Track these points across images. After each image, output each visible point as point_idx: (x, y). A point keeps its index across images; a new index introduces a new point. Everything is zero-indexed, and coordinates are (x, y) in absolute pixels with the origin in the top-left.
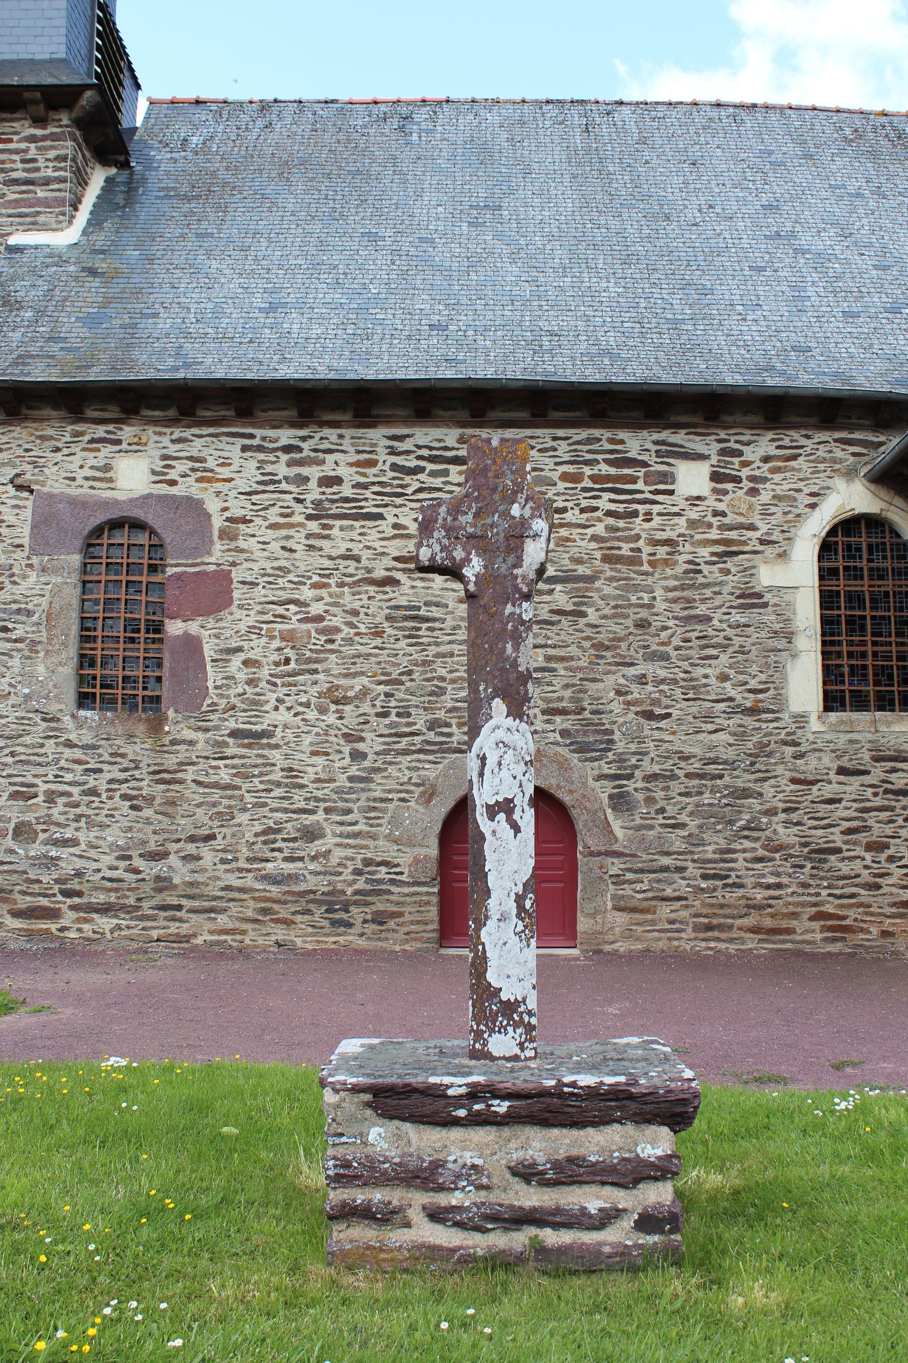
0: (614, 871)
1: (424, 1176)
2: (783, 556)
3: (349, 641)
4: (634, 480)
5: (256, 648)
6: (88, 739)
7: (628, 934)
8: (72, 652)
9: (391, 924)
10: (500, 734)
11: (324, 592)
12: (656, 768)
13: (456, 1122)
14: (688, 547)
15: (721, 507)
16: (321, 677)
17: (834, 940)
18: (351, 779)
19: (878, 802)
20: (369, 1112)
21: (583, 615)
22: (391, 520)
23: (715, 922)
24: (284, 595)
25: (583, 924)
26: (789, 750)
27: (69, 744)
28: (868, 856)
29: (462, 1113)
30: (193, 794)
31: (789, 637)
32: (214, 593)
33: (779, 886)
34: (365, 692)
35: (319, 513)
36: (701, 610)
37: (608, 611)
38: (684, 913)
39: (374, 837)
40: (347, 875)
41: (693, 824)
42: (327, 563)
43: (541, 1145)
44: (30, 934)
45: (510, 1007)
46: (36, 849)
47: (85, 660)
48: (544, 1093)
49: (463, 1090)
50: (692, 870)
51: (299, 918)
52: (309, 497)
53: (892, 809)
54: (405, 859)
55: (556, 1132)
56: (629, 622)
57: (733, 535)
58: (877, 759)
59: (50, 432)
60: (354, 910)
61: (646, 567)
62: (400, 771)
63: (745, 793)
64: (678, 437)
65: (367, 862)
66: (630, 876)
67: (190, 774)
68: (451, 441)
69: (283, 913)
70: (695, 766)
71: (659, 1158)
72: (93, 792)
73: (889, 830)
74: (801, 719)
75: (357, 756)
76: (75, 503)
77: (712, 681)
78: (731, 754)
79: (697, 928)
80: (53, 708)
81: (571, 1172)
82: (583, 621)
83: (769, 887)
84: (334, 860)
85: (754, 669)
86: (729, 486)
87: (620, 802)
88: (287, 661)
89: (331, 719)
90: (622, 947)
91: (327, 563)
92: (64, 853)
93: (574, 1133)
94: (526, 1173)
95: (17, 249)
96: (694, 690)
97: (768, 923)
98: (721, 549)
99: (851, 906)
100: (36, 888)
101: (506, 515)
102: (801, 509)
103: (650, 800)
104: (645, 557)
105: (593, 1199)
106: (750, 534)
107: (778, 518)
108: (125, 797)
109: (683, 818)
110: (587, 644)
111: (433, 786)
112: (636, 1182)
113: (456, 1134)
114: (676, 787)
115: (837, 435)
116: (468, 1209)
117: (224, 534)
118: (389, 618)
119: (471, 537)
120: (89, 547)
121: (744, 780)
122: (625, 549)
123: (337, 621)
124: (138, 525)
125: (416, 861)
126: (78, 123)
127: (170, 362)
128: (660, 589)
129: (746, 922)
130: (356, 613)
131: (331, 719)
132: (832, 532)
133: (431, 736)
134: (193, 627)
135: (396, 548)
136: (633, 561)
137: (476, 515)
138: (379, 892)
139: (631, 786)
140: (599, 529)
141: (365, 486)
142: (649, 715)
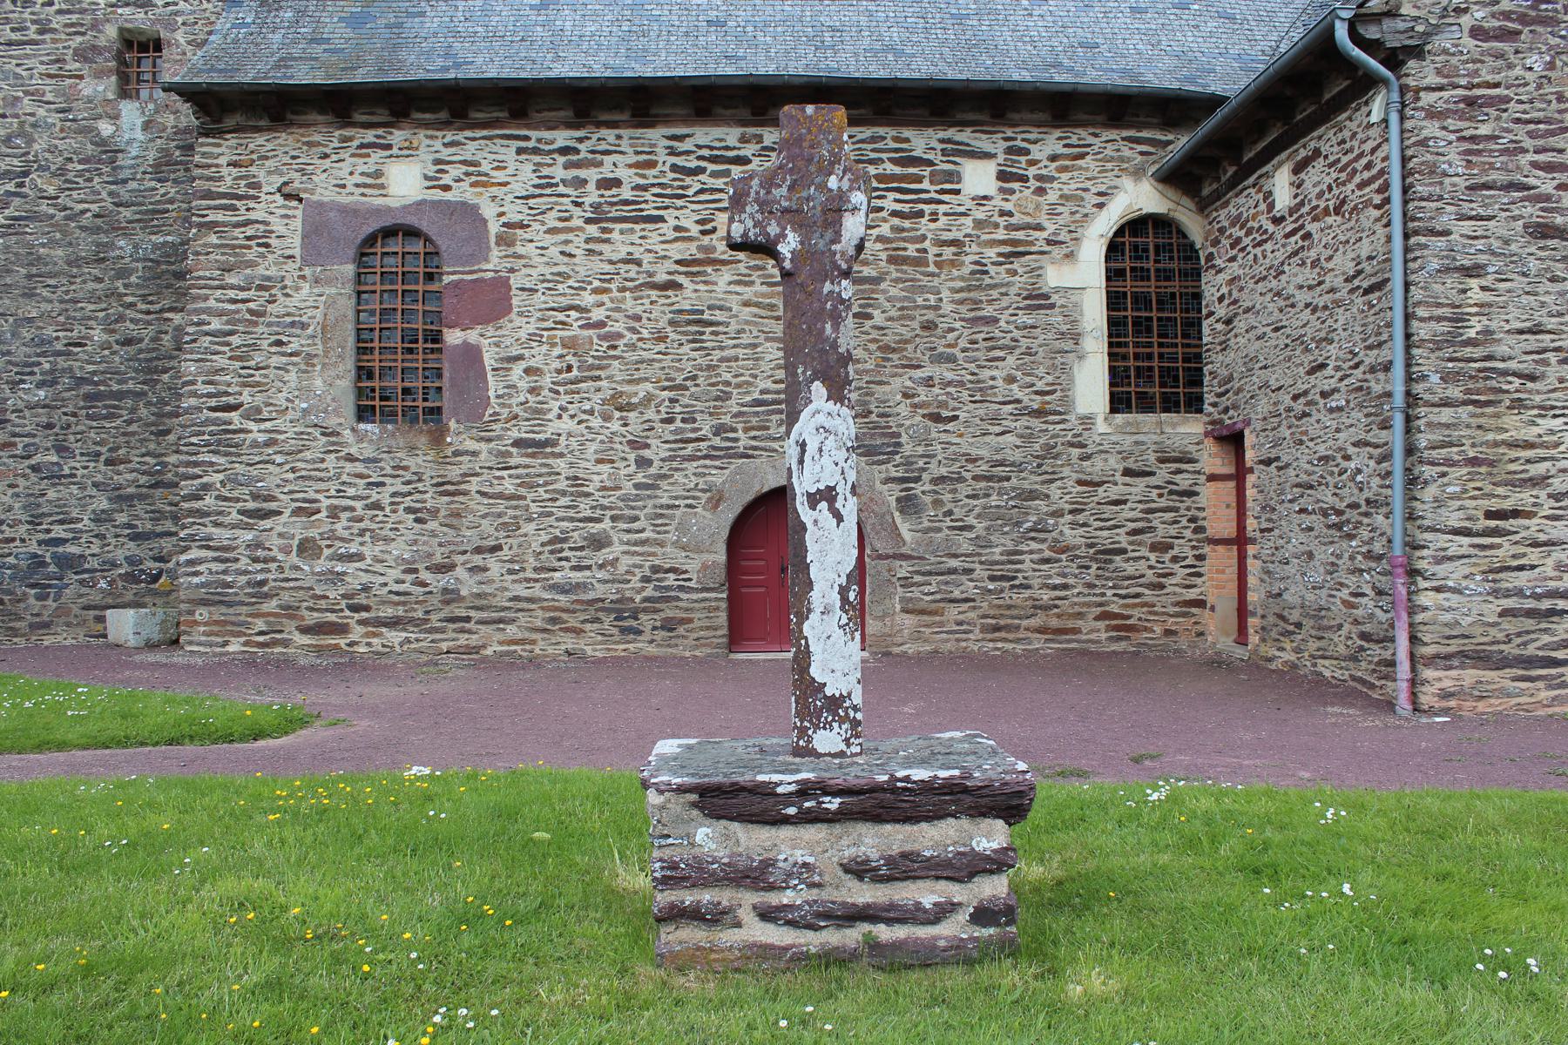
0: (902, 573)
1: (755, 876)
2: (1070, 256)
3: (632, 347)
4: (919, 179)
5: (538, 356)
6: (369, 452)
7: (917, 636)
8: (349, 364)
9: (681, 630)
10: (821, 419)
11: (605, 298)
12: (944, 471)
13: (786, 820)
14: (975, 248)
15: (1008, 206)
16: (604, 383)
17: (1119, 639)
18: (637, 486)
19: (1163, 503)
20: (695, 812)
21: (869, 317)
22: (672, 222)
23: (1002, 622)
24: (565, 301)
26: (1076, 452)
27: (350, 458)
28: (1153, 557)
29: (792, 811)
30: (478, 505)
31: (1076, 338)
32: (492, 301)
33: (1065, 587)
34: (649, 398)
35: (598, 216)
36: (988, 311)
37: (894, 313)
38: (972, 615)
39: (661, 544)
40: (635, 582)
41: (980, 527)
42: (608, 268)
43: (873, 841)
44: (319, 650)
45: (835, 703)
46: (321, 565)
47: (363, 373)
48: (876, 789)
49: (792, 788)
50: (980, 572)
51: (588, 626)
52: (588, 200)
53: (1176, 510)
55: (888, 827)
56: (915, 324)
57: (1020, 235)
58: (1162, 461)
59: (317, 138)
60: (643, 617)
61: (932, 268)
62: (687, 477)
63: (1032, 495)
64: (964, 135)
65: (656, 569)
66: (918, 578)
67: (474, 485)
68: (732, 141)
69: (573, 622)
71: (995, 851)
72: (377, 506)
73: (1173, 531)
74: (1087, 421)
75: (643, 463)
76: (344, 210)
77: (999, 383)
78: (1017, 456)
79: (984, 629)
80: (332, 422)
81: (905, 867)
82: (869, 323)
83: (1055, 587)
84: (622, 568)
85: (1041, 371)
86: (1016, 185)
87: (908, 505)
88: (569, 368)
89: (615, 426)
90: (910, 648)
91: (608, 268)
92: (350, 567)
93: (908, 828)
94: (858, 870)
96: (981, 393)
97: (1054, 623)
98: (1008, 249)
99: (1135, 606)
100: (323, 604)
101: (823, 187)
102: (1089, 209)
103: (937, 503)
104: (931, 258)
105: (927, 894)
106: (1037, 234)
107: (1065, 218)
108: (409, 510)
109: (971, 520)
110: (873, 347)
111: (720, 492)
112: (972, 875)
113: (786, 832)
114: (964, 489)
115: (1125, 133)
116: (799, 907)
117: (502, 240)
118: (672, 323)
119: (786, 211)
120: (363, 254)
121: (1031, 482)
123: (618, 327)
124: (412, 233)
125: (705, 567)
127: (440, 62)
128: (946, 290)
129: (1033, 622)
130: (638, 318)
131: (615, 426)
132: (1120, 232)
133: (717, 441)
134: (472, 336)
135: (677, 251)
136: (919, 262)
137: (791, 188)
138: (668, 599)
139: (918, 488)
141: (644, 188)
142: (936, 418)
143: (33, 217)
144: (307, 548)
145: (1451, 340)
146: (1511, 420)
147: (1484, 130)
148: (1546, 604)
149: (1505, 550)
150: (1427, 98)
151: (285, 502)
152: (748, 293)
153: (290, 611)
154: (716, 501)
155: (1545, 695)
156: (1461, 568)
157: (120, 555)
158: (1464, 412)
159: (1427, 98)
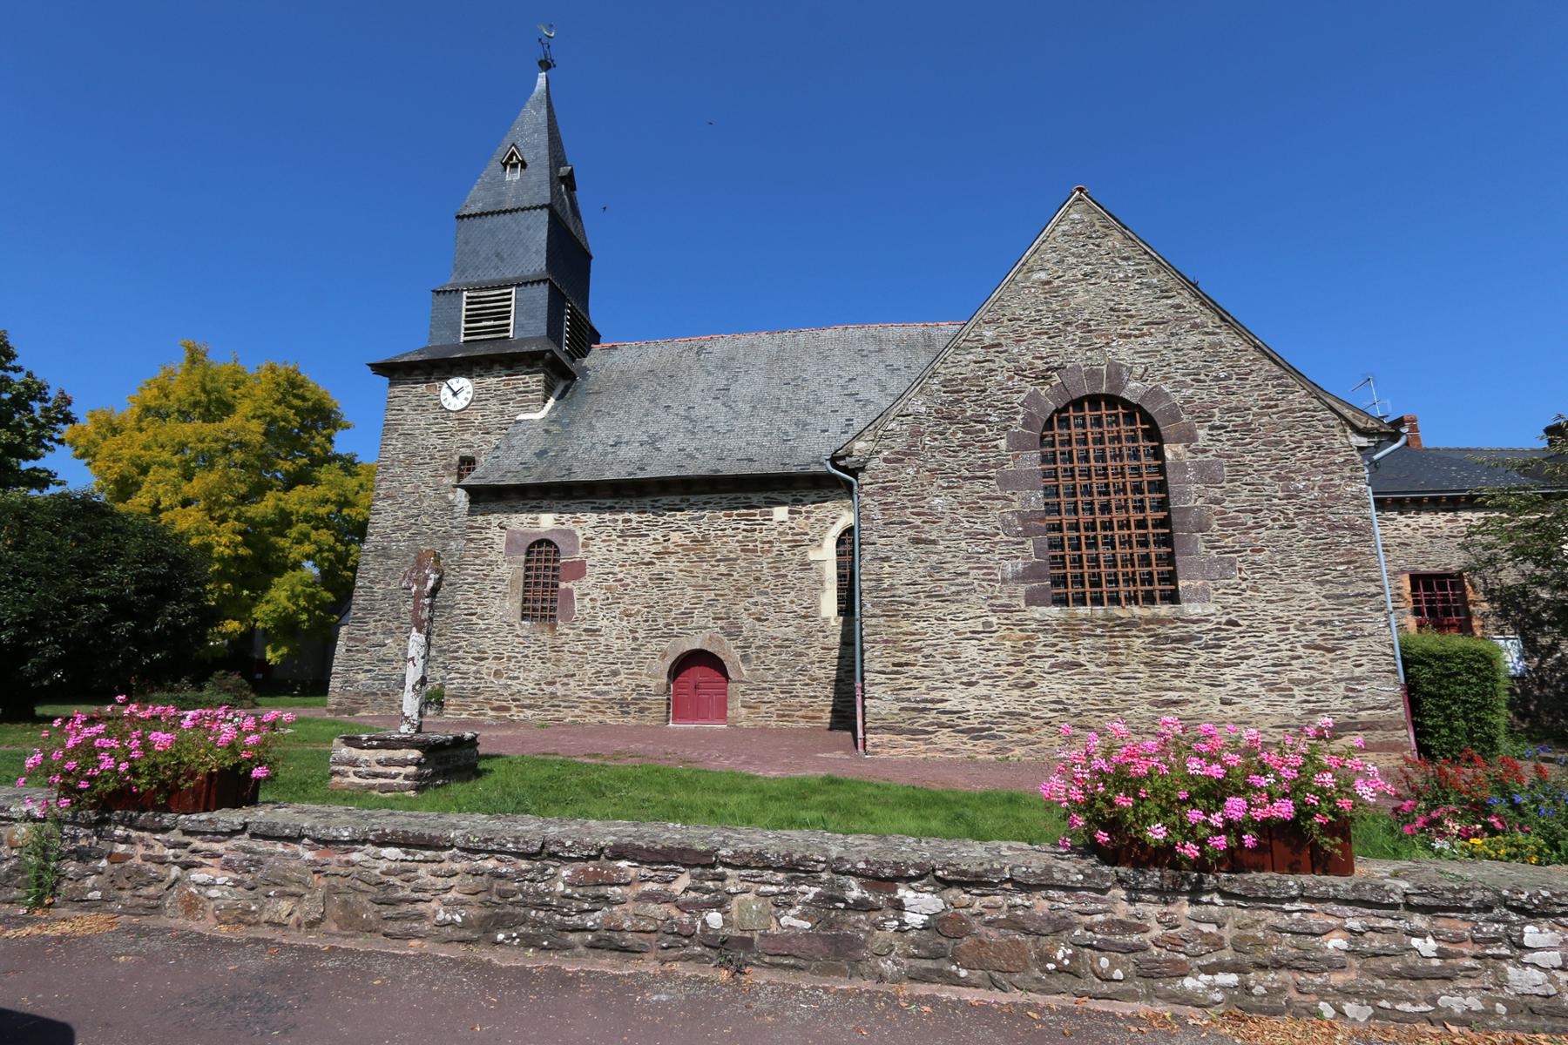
1: (353, 763)
5: (595, 593)
7: (748, 718)
25: (729, 713)
30: (568, 656)
32: (578, 570)
35: (623, 534)
36: (783, 572)
41: (777, 668)
43: (384, 754)
46: (503, 681)
47: (525, 600)
50: (777, 689)
54: (653, 684)
63: (801, 655)
64: (775, 495)
67: (566, 648)
70: (778, 642)
74: (826, 620)
75: (635, 639)
76: (522, 533)
78: (794, 637)
87: (745, 658)
90: (745, 724)
94: (379, 762)
95: (520, 422)
96: (779, 608)
105: (394, 770)
114: (770, 651)
117: (585, 545)
120: (528, 553)
121: (801, 648)
122: (751, 546)
124: (549, 543)
126: (546, 365)
128: (765, 561)
132: (843, 534)
134: (570, 585)
135: (653, 549)
136: (754, 551)
139: (750, 651)
140: (740, 537)
142: (759, 620)
143: (420, 533)
144: (497, 674)
145: (876, 589)
146: (903, 623)
147: (890, 500)
148: (921, 705)
149: (902, 680)
150: (866, 488)
151: (490, 654)
152: (682, 566)
153: (488, 701)
154: (664, 655)
155: (923, 747)
156: (881, 689)
157: (438, 676)
158: (882, 620)
159: (866, 488)
